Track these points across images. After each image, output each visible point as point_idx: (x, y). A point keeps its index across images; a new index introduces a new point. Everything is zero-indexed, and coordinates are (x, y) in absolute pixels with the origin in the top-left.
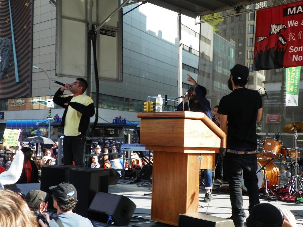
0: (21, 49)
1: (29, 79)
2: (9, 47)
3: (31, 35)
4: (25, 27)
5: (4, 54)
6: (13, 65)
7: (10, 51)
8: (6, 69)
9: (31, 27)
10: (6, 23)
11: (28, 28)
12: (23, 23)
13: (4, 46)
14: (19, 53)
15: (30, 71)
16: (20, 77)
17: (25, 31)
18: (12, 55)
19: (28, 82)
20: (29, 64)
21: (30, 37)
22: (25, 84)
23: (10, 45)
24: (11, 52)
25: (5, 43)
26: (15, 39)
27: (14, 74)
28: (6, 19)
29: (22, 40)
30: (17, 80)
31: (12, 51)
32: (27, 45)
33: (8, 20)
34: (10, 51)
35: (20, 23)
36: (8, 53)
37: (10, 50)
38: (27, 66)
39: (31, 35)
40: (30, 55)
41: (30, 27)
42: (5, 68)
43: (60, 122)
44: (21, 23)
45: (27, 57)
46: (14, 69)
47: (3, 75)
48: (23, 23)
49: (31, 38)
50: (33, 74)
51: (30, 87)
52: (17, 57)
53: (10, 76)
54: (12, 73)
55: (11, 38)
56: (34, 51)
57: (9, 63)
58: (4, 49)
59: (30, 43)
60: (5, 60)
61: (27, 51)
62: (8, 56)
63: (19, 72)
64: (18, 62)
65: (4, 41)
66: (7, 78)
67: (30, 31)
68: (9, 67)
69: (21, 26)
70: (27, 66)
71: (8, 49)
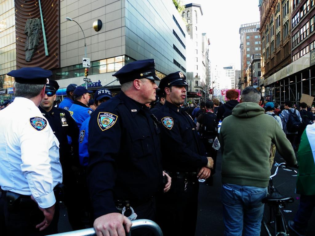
0: (49, 26)
1: (57, 52)
2: (38, 26)
3: (58, 11)
4: (52, 5)
5: (34, 32)
6: (43, 41)
7: (39, 29)
8: (36, 46)
9: (58, 4)
10: (35, 6)
11: (56, 5)
12: (51, 2)
13: (34, 25)
14: (48, 30)
15: (58, 44)
16: (49, 51)
17: (53, 9)
18: (42, 33)
19: (57, 54)
20: (57, 38)
21: (57, 13)
22: (54, 57)
23: (39, 24)
24: (40, 30)
25: (35, 22)
26: (44, 18)
27: (44, 50)
28: (35, 3)
29: (49, 19)
30: (47, 54)
31: (41, 29)
32: (56, 20)
33: (37, 3)
34: (39, 29)
35: (48, 3)
36: (38, 31)
37: (40, 28)
38: (55, 40)
39: (58, 11)
40: (58, 30)
41: (57, 5)
42: (35, 45)
43: (92, 87)
44: (49, 3)
45: (55, 32)
46: (44, 45)
47: (34, 52)
48: (51, 2)
49: (58, 14)
50: (61, 46)
51: (58, 59)
52: (46, 34)
53: (40, 52)
54: (42, 48)
55: (40, 18)
56: (61, 25)
57: (39, 40)
58: (33, 27)
59: (58, 19)
60: (35, 38)
61: (55, 27)
62: (38, 34)
63: (48, 46)
64: (47, 38)
65: (33, 21)
66: (38, 54)
67: (58, 8)
68: (39, 43)
69: (49, 5)
70: (55, 40)
71: (37, 27)
